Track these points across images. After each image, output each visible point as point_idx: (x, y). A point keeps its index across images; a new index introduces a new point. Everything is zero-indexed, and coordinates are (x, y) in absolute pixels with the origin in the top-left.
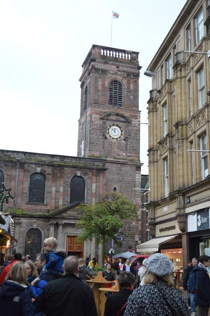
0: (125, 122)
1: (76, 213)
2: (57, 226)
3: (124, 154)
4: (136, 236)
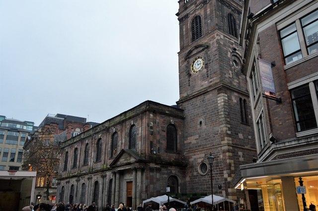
0: (203, 50)
1: (123, 160)
2: (115, 173)
3: (206, 82)
4: (225, 172)
